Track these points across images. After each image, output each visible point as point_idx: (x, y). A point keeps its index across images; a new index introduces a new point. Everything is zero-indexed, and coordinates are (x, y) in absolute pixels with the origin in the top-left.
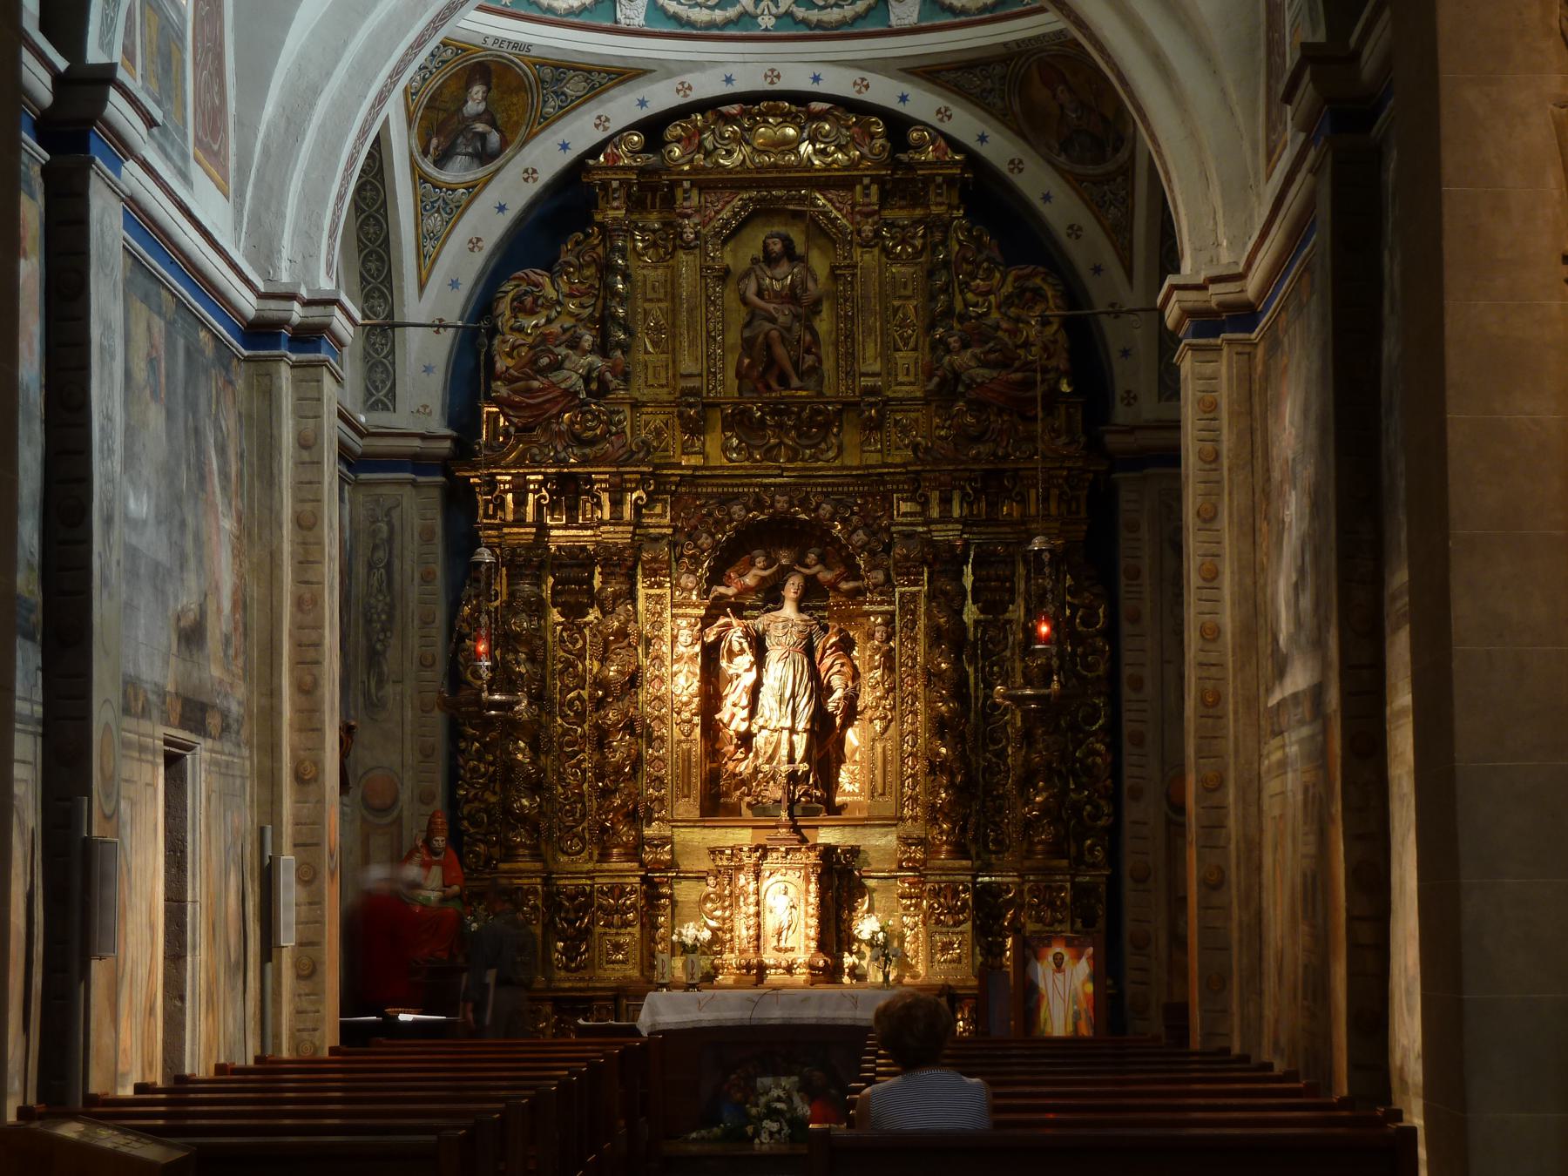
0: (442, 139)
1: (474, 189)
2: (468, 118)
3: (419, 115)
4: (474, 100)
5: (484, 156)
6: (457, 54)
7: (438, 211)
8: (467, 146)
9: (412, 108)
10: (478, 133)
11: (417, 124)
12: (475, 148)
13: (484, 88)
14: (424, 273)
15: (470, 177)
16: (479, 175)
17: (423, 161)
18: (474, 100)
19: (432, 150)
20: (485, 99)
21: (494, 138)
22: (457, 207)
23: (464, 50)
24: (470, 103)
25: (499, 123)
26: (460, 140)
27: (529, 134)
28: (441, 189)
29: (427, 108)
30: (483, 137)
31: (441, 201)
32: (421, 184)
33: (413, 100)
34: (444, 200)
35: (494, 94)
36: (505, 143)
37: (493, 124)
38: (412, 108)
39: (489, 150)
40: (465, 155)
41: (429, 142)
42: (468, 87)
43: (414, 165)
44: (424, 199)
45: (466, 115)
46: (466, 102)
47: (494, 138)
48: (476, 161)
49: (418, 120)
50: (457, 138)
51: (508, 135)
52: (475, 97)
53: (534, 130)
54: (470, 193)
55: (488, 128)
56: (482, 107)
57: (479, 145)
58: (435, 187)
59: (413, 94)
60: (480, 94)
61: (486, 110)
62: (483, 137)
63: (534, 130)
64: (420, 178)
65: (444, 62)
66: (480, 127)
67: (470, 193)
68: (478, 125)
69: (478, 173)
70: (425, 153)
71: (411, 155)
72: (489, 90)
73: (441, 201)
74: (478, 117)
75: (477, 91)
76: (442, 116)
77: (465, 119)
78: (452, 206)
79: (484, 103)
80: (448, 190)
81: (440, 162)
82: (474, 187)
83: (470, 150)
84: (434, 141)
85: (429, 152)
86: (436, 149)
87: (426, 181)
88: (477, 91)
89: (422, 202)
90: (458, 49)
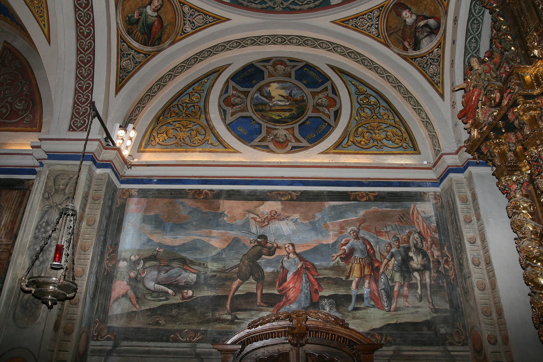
0: (409, 40)
1: (441, 46)
2: (412, 25)
3: (389, 40)
4: (408, 17)
5: (434, 31)
6: (381, 11)
7: (431, 64)
8: (423, 34)
9: (383, 41)
10: (423, 26)
11: (391, 44)
12: (427, 32)
13: (407, 10)
14: (440, 90)
15: (435, 43)
16: (438, 39)
17: (408, 53)
18: (408, 17)
19: (408, 47)
20: (412, 13)
21: (432, 22)
22: (439, 57)
23: (382, 7)
24: (407, 20)
25: (428, 15)
26: (417, 34)
27: (444, 8)
28: (425, 56)
29: (389, 35)
30: (426, 25)
31: (429, 60)
32: (414, 61)
33: (380, 38)
34: (430, 59)
35: (413, 9)
36: (438, 20)
37: (426, 18)
38: (383, 41)
39: (434, 28)
40: (425, 37)
41: (403, 44)
42: (399, 15)
43: (405, 58)
44: (420, 65)
45: (410, 25)
46: (405, 21)
47: (432, 22)
48: (433, 36)
49: (390, 43)
50: (415, 34)
51: (438, 16)
52: (407, 16)
53: (445, 4)
54: (440, 48)
55: (425, 21)
56: (414, 17)
57: (427, 29)
58: (422, 57)
59: (377, 36)
60: (408, 14)
61: (418, 16)
62: (426, 25)
63: (445, 4)
64: (412, 59)
65: (378, 17)
66: (422, 23)
67: (440, 48)
68: (420, 24)
69: (438, 38)
70: (405, 49)
71: (399, 55)
72: (410, 9)
73: (429, 60)
74: (416, 21)
75: (405, 14)
76: (400, 33)
77: (411, 27)
78: (436, 58)
79: (414, 15)
80: (429, 54)
81: (416, 46)
82: (440, 44)
83: (425, 34)
84: (406, 44)
85: (407, 48)
86: (409, 45)
87: (415, 59)
88: (405, 14)
89: (420, 66)
90: (379, 8)
